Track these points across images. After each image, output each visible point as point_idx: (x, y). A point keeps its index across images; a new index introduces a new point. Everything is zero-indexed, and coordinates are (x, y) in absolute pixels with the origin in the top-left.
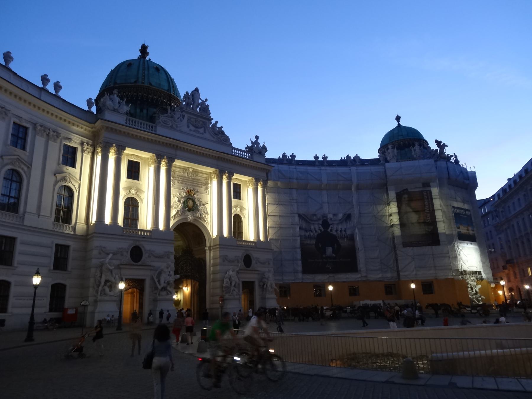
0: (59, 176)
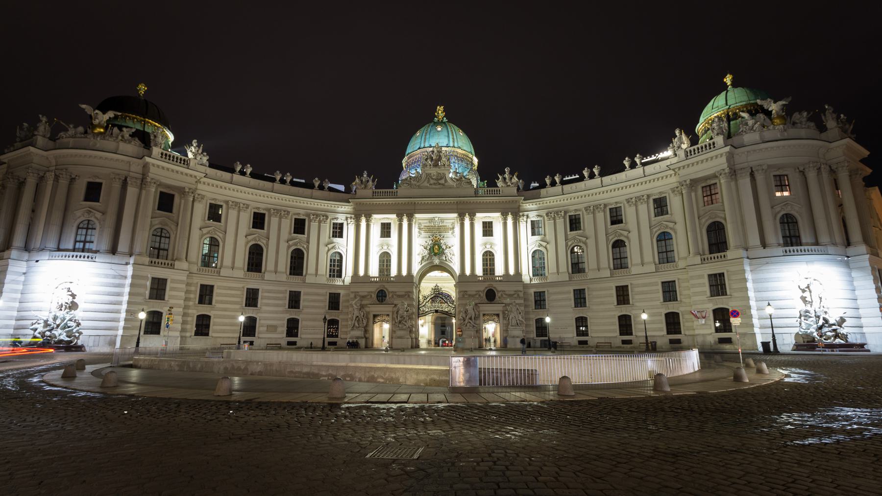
0: (330, 246)
